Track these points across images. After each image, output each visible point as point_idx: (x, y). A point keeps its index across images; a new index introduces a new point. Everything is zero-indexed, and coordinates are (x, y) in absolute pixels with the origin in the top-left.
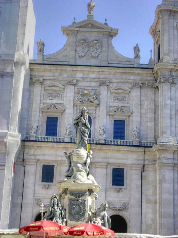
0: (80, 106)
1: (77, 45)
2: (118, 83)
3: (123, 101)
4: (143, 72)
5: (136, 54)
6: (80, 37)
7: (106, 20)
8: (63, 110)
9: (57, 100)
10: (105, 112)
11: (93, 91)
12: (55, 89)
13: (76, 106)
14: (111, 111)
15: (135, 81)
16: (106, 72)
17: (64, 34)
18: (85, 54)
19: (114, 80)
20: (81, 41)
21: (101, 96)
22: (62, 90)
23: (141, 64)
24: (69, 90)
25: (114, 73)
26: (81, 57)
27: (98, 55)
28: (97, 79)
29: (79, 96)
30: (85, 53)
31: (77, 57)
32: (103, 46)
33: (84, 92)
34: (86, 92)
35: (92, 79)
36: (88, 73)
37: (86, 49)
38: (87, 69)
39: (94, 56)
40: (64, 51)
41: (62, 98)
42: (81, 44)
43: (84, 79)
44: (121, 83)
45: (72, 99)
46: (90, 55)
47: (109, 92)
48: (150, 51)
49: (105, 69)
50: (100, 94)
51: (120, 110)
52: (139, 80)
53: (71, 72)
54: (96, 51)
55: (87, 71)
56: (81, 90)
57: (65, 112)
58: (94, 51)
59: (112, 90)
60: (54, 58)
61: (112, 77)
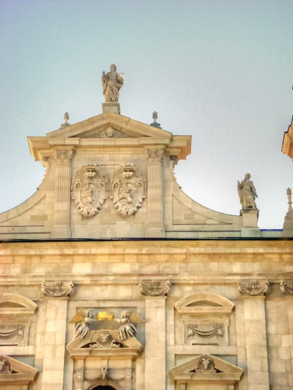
0: (85, 360)
1: (75, 186)
2: (199, 284)
3: (214, 340)
4: (270, 250)
5: (245, 202)
6: (81, 162)
7: (155, 116)
8: (35, 373)
9: (16, 345)
10: (162, 374)
11: (124, 313)
12: (9, 313)
13: (75, 360)
14: (179, 370)
15: (246, 278)
16: (161, 254)
17: (37, 159)
18: (98, 209)
19: (182, 278)
20: (87, 174)
21: (148, 328)
22: (31, 315)
23: (262, 230)
24: (51, 314)
25: (184, 257)
26: (87, 217)
27: (135, 209)
28: (135, 278)
29: (80, 329)
30: (100, 206)
31: (76, 217)
32: (149, 184)
33: (97, 315)
34: (102, 315)
35: (119, 278)
36: (107, 261)
37: (102, 196)
38: (105, 249)
39: (124, 212)
40: (37, 204)
41: (31, 340)
42: (87, 181)
43: (95, 279)
44: (205, 284)
45: (60, 338)
46: (113, 211)
47: (173, 310)
48: (285, 192)
49: (155, 246)
50: (144, 321)
51: (206, 367)
52: (259, 275)
53: (57, 260)
54: (129, 199)
55: (102, 255)
56: (87, 311)
57: (39, 381)
58: (123, 198)
59: (180, 306)
60: (7, 224)
61: (177, 270)
